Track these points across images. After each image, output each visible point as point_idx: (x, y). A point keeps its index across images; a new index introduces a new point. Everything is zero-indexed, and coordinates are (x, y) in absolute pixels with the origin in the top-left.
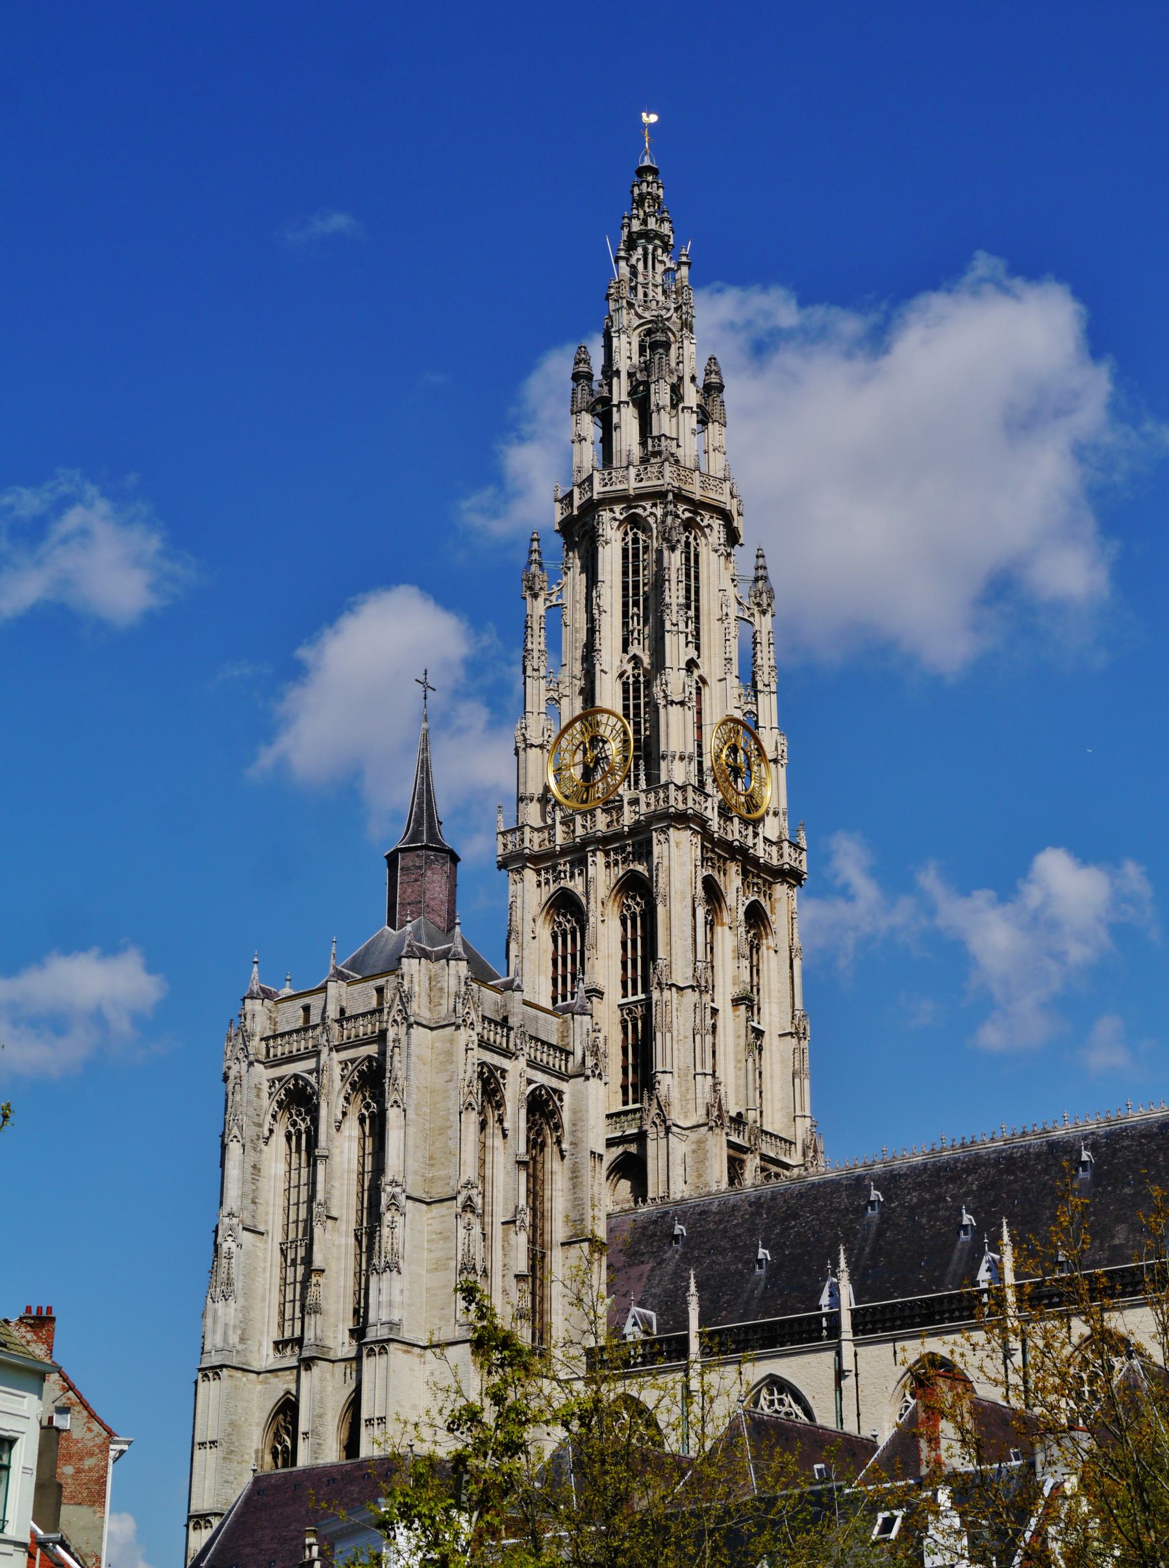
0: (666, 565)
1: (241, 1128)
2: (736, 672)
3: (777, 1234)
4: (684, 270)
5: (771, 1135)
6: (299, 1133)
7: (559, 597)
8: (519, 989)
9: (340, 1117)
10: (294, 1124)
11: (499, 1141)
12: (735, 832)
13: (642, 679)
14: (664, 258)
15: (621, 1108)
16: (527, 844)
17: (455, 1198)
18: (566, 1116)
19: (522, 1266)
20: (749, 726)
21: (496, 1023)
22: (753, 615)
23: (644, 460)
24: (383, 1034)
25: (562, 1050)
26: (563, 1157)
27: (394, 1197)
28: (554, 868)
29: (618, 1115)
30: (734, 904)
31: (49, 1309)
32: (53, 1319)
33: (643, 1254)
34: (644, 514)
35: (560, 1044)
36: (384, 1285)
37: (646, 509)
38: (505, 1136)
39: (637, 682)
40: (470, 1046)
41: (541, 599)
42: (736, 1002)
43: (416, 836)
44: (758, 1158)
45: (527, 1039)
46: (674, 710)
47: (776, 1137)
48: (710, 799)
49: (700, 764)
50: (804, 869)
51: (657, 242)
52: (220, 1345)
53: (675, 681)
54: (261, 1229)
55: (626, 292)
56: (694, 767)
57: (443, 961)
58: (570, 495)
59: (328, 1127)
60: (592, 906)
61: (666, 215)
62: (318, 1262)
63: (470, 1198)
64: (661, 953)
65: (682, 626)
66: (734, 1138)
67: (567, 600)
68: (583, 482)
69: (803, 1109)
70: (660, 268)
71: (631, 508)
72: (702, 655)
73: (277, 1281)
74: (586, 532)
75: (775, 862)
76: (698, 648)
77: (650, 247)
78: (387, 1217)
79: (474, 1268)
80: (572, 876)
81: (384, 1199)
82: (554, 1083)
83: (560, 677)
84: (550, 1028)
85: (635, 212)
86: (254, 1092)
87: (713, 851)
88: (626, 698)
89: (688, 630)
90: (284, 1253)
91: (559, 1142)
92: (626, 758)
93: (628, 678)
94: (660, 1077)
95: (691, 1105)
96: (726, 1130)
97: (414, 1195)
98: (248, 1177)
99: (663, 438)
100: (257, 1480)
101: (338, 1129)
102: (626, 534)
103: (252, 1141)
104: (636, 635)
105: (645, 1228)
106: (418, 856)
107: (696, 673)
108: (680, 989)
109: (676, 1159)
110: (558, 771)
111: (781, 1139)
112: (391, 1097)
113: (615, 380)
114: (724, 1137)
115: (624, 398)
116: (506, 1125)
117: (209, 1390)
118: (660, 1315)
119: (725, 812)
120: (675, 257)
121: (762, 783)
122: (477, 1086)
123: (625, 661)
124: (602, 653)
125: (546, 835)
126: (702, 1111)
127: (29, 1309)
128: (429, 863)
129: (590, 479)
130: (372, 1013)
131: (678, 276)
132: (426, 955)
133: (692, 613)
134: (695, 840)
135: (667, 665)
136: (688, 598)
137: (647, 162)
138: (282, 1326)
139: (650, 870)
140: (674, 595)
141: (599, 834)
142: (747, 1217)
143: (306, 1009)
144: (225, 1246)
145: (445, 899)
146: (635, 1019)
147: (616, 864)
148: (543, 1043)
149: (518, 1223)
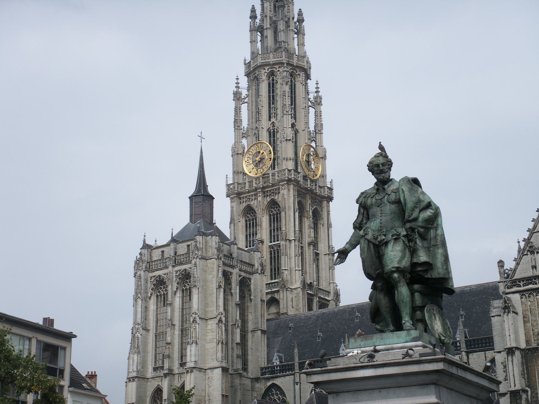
3: (324, 328)
8: (236, 244)
9: (175, 290)
11: (230, 297)
18: (252, 287)
19: (238, 339)
21: (228, 257)
26: (251, 301)
30: (308, 210)
31: (95, 372)
33: (279, 334)
34: (276, 71)
38: (232, 295)
40: (220, 266)
44: (318, 298)
45: (239, 261)
47: (324, 290)
48: (300, 174)
65: (290, 113)
72: (297, 121)
75: (323, 194)
76: (295, 119)
82: (248, 276)
84: (245, 257)
91: (250, 295)
93: (271, 130)
99: (282, 42)
103: (145, 298)
104: (273, 115)
105: (279, 324)
106: (200, 198)
108: (290, 241)
111: (325, 291)
115: (269, 26)
118: (285, 355)
123: (270, 124)
127: (88, 372)
133: (293, 106)
142: (314, 321)
146: (275, 250)
147: (267, 196)
149: (237, 325)
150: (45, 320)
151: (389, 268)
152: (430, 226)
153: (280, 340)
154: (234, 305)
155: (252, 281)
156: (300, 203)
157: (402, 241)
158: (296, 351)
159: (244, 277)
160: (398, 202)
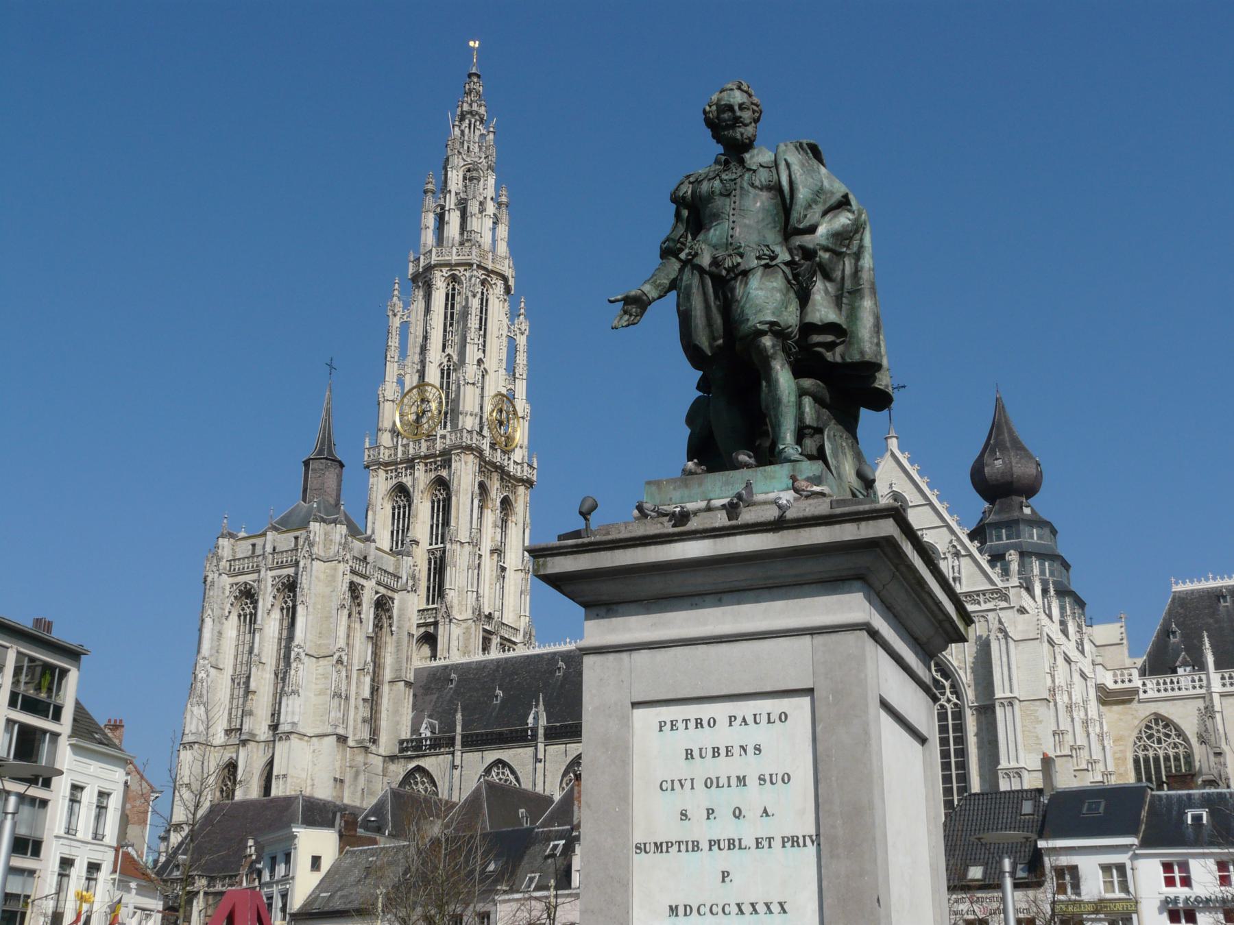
0: (470, 305)
1: (212, 610)
2: (504, 366)
4: (491, 136)
5: (507, 625)
6: (245, 616)
7: (408, 317)
8: (374, 541)
9: (270, 607)
10: (243, 609)
11: (357, 625)
12: (498, 457)
13: (452, 368)
14: (480, 127)
15: (425, 607)
16: (381, 456)
17: (332, 656)
18: (395, 612)
19: (366, 693)
20: (509, 398)
21: (360, 560)
22: (516, 335)
23: (462, 244)
24: (297, 563)
25: (395, 576)
26: (392, 634)
27: (298, 654)
28: (396, 470)
29: (423, 610)
31: (121, 721)
32: (123, 726)
34: (459, 275)
35: (395, 572)
36: (290, 702)
37: (460, 272)
38: (361, 622)
39: (449, 369)
41: (398, 317)
42: (493, 551)
43: (321, 452)
46: (469, 387)
47: (509, 626)
49: (481, 418)
50: (535, 479)
51: (477, 117)
52: (193, 731)
53: (471, 371)
54: (221, 667)
55: (457, 145)
56: (478, 418)
57: (333, 525)
58: (419, 259)
59: (263, 613)
60: (416, 494)
61: (483, 102)
62: (253, 686)
63: (340, 656)
64: (453, 523)
65: (476, 341)
66: (487, 627)
67: (413, 319)
68: (426, 253)
69: (525, 611)
70: (477, 133)
71: (451, 270)
73: (228, 696)
74: (426, 281)
75: (519, 474)
76: (484, 352)
77: (473, 120)
78: (294, 665)
79: (341, 695)
80: (406, 475)
81: (293, 655)
82: (390, 593)
83: (406, 362)
84: (389, 563)
85: (466, 99)
86: (221, 590)
87: (485, 467)
88: (442, 377)
89: (480, 342)
90: (233, 680)
91: (391, 626)
92: (440, 412)
94: (447, 591)
95: (464, 608)
96: (482, 622)
97: (310, 653)
98: (215, 638)
100: (212, 806)
101: (268, 613)
102: (448, 284)
107: (482, 366)
109: (454, 637)
110: (402, 415)
111: (512, 628)
112: (299, 599)
113: (448, 195)
114: (481, 626)
116: (362, 616)
117: (186, 756)
118: (440, 723)
119: (493, 446)
120: (487, 128)
121: (514, 430)
122: (348, 594)
124: (431, 351)
125: (393, 452)
126: (470, 611)
127: (110, 721)
128: (327, 467)
129: (430, 251)
130: (292, 550)
131: (487, 138)
132: (323, 520)
133: (482, 332)
134: (475, 461)
135: (467, 362)
136: (481, 323)
137: (474, 70)
138: (230, 721)
139: (450, 475)
140: (473, 322)
141: (422, 454)
143: (254, 545)
144: (200, 676)
145: (335, 488)
147: (431, 470)
148: (385, 571)
150: (38, 622)
151: (750, 324)
152: (844, 249)
153: (434, 700)
154: (364, 639)
155: (396, 602)
156: (482, 486)
157: (781, 274)
158: (459, 716)
159: (383, 596)
160: (776, 188)
